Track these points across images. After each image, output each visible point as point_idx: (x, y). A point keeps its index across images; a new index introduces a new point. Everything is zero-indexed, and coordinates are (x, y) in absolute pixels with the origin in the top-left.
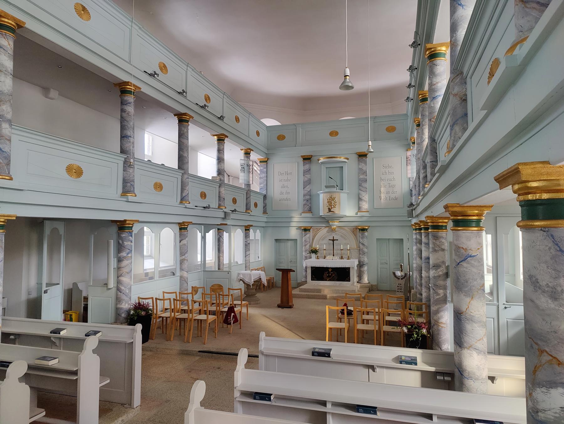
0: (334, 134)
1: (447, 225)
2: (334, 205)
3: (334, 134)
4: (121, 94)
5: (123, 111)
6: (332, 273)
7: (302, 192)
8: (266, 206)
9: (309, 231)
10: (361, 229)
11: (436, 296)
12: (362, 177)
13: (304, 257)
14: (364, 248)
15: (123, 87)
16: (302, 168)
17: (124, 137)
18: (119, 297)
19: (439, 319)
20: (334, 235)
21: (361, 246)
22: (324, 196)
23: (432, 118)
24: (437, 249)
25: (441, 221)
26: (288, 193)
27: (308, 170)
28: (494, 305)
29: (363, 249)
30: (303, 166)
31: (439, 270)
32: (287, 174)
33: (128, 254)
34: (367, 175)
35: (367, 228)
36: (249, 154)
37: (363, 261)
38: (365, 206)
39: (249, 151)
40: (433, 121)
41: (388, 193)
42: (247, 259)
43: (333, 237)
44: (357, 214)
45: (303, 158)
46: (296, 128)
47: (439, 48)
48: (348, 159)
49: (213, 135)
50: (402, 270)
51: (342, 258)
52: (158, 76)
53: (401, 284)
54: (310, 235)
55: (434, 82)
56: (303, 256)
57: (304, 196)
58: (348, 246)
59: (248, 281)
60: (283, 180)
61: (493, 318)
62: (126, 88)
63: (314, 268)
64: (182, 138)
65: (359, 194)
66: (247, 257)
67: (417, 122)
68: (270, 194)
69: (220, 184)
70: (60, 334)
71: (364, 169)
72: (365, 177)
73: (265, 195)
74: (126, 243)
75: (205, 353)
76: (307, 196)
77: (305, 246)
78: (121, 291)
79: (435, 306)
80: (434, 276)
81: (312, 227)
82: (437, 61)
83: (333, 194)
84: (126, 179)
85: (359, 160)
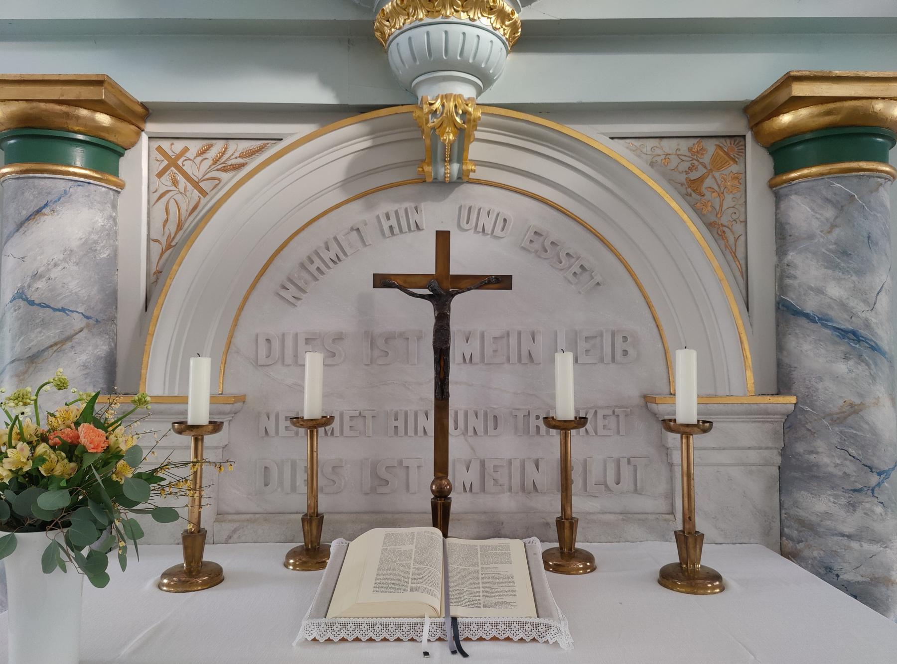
29: (855, 410)
43: (443, 238)
81: (152, 127)
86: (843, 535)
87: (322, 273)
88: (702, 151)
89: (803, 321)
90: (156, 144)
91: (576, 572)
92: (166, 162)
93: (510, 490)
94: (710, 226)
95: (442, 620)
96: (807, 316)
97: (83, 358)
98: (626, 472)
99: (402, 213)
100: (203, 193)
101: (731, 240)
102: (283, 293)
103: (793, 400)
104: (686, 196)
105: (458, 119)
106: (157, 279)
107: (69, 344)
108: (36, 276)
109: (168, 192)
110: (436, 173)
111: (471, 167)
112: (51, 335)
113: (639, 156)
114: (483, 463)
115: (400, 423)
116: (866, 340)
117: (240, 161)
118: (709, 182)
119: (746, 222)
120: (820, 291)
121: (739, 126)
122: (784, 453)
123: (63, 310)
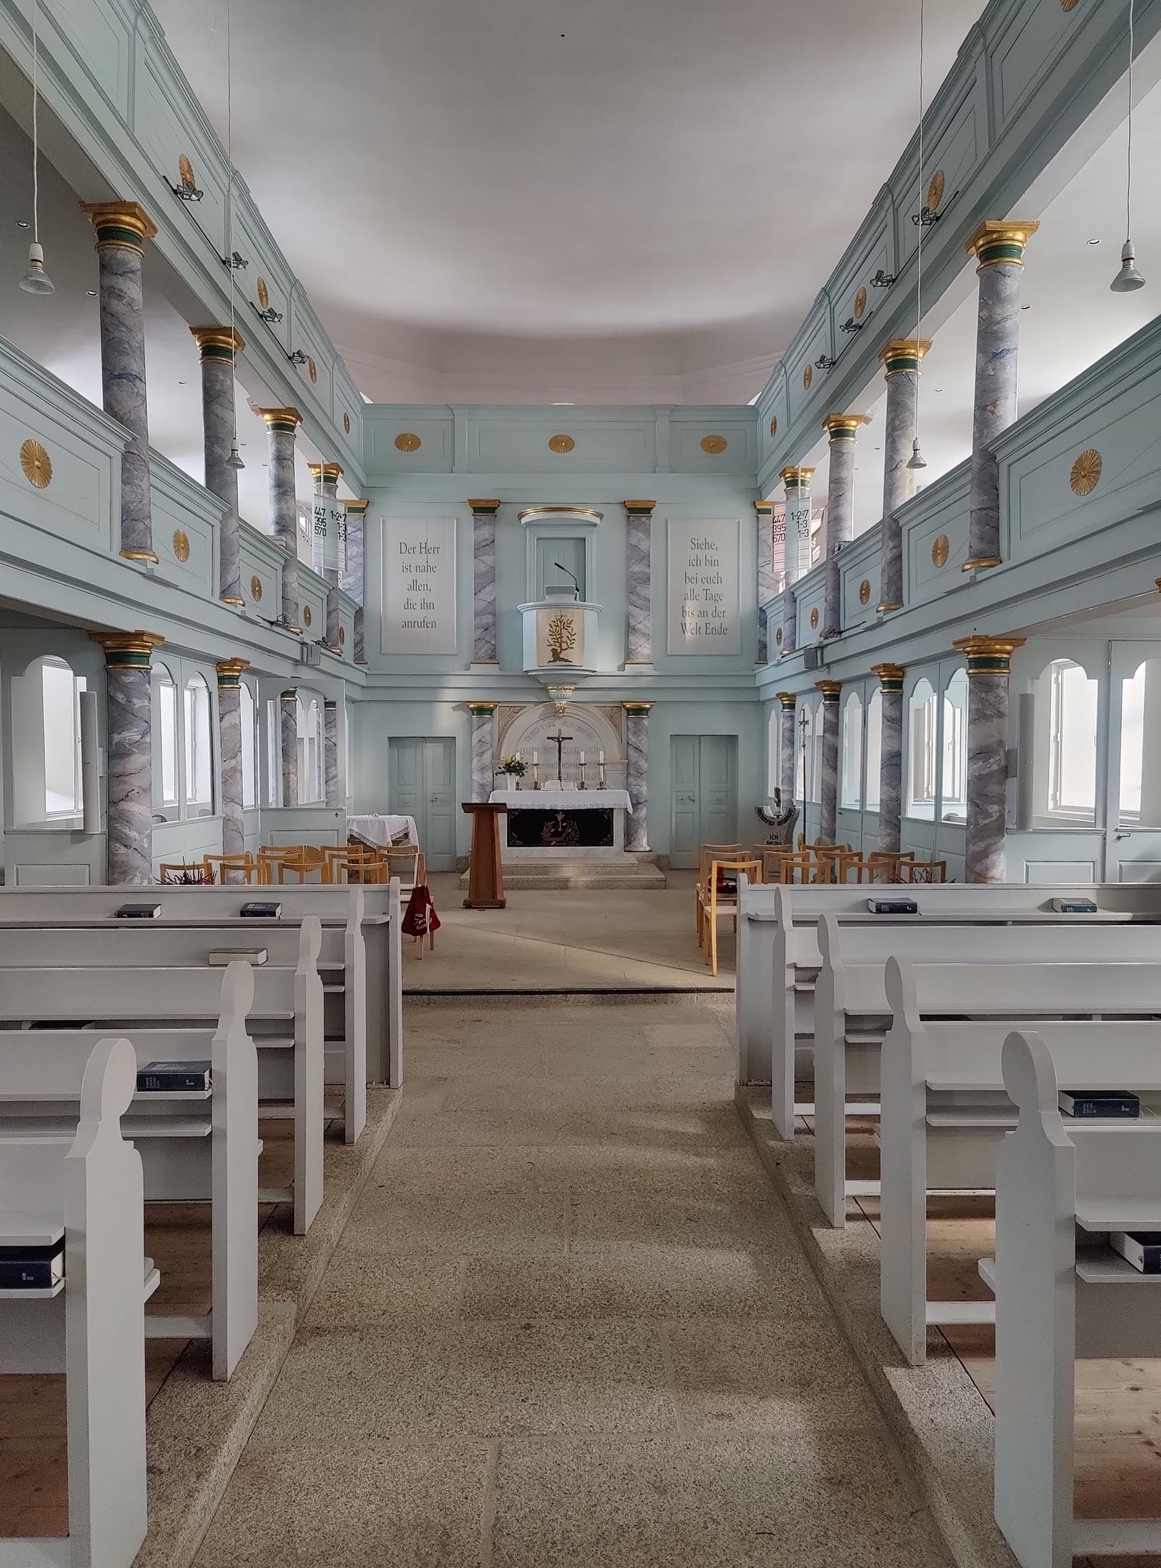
0: (561, 443)
1: (1009, 659)
3: (561, 443)
4: (100, 240)
5: (109, 294)
6: (564, 824)
7: (470, 605)
8: (361, 641)
9: (491, 714)
10: (633, 710)
11: (981, 818)
12: (636, 568)
14: (641, 758)
15: (112, 216)
16: (471, 536)
17: (120, 377)
18: (122, 862)
19: (987, 869)
20: (559, 724)
21: (633, 754)
22: (540, 618)
23: (988, 403)
24: (989, 712)
25: (998, 647)
26: (430, 606)
27: (488, 542)
28: (1095, 833)
30: (475, 529)
31: (992, 761)
32: (425, 548)
33: (143, 735)
34: (649, 565)
35: (648, 706)
36: (334, 480)
37: (639, 793)
38: (644, 649)
39: (334, 474)
40: (990, 411)
41: (703, 614)
42: (332, 789)
43: (560, 730)
44: (622, 668)
45: (474, 508)
46: (452, 418)
47: (1010, 235)
48: (600, 516)
49: (261, 409)
50: (779, 801)
51: (582, 786)
52: (199, 200)
53: (777, 837)
54: (491, 726)
55: (996, 316)
56: (475, 783)
57: (477, 614)
58: (602, 753)
59: (376, 842)
60: (413, 569)
61: (1094, 862)
62: (118, 223)
63: (517, 813)
64: (218, 406)
65: (628, 617)
66: (331, 783)
67: (833, 424)
68: (374, 606)
69: (286, 560)
70: (151, 915)
71: (643, 546)
72: (646, 570)
73: (361, 609)
74: (137, 703)
75: (409, 997)
77: (481, 756)
78: (129, 843)
79: (979, 843)
80: (980, 775)
81: (499, 705)
82: (1006, 266)
83: (566, 610)
84: (132, 508)
85: (629, 523)
112: (486, 748)
120: (631, 740)
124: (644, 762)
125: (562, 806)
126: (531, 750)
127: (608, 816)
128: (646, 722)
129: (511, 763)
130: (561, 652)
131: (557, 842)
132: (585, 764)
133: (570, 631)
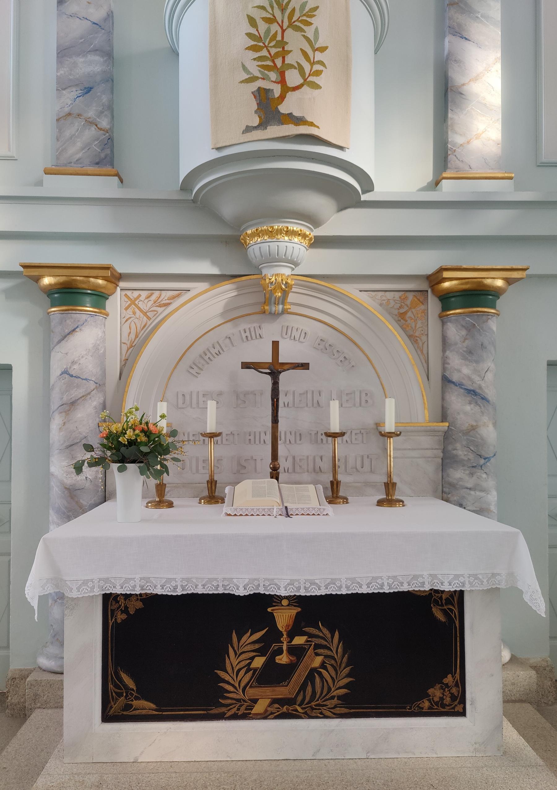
2: (307, 72)
6: (299, 640)
13: (56, 491)
14: (485, 419)
29: (473, 428)
35: (499, 283)
43: (276, 345)
58: (390, 405)
63: (134, 606)
76: (84, 53)
81: (122, 284)
86: (467, 488)
87: (211, 360)
88: (406, 298)
89: (452, 385)
90: (124, 293)
91: (339, 503)
92: (129, 302)
93: (308, 471)
94: (410, 337)
95: (281, 507)
96: (453, 383)
97: (95, 403)
98: (367, 462)
99: (252, 330)
100: (149, 318)
101: (421, 344)
102: (191, 370)
103: (447, 424)
104: (398, 321)
105: (283, 287)
106: (126, 363)
107: (89, 396)
108: (73, 363)
109: (130, 318)
110: (271, 310)
111: (288, 307)
112: (80, 392)
113: (374, 300)
114: (294, 458)
115: (252, 438)
116: (479, 395)
117: (168, 301)
118: (409, 314)
119: (427, 335)
120: (459, 371)
121: (424, 286)
122: (444, 451)
123: (86, 379)
124: (491, 428)
125: (291, 583)
126: (201, 399)
127: (445, 612)
128: (493, 324)
129: (124, 433)
130: (282, 98)
131: (274, 701)
132: (342, 434)
133: (311, 35)
